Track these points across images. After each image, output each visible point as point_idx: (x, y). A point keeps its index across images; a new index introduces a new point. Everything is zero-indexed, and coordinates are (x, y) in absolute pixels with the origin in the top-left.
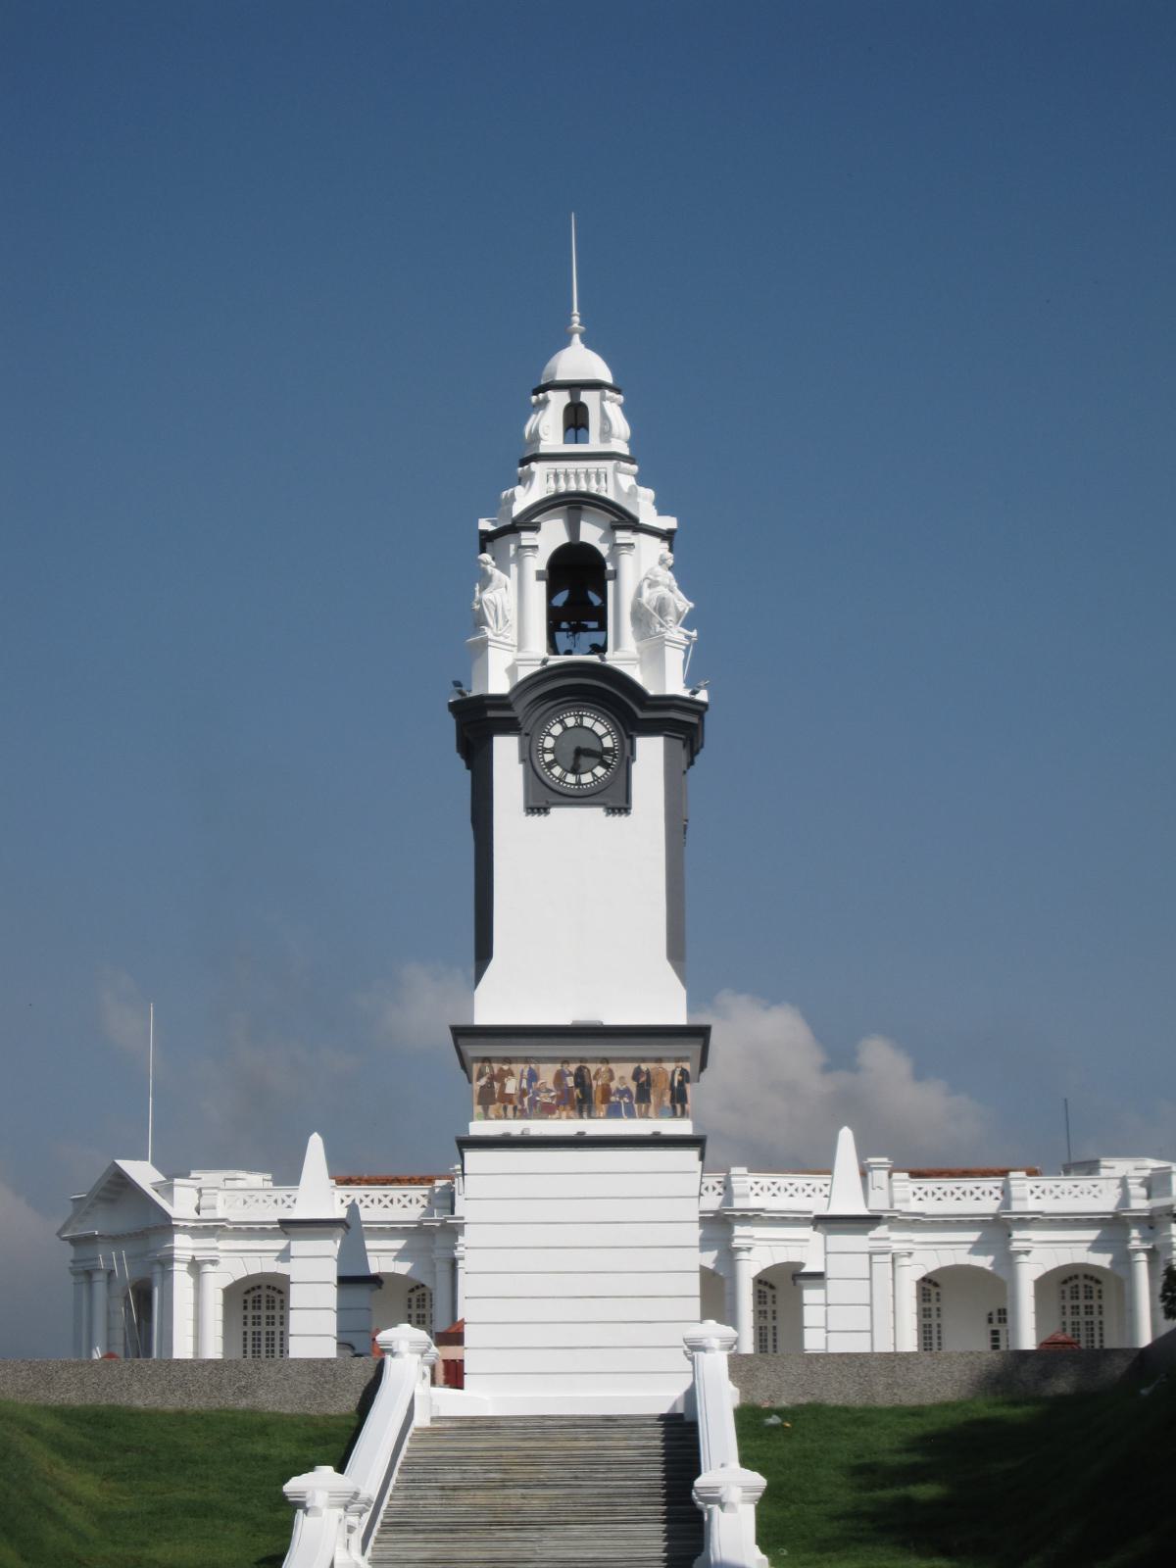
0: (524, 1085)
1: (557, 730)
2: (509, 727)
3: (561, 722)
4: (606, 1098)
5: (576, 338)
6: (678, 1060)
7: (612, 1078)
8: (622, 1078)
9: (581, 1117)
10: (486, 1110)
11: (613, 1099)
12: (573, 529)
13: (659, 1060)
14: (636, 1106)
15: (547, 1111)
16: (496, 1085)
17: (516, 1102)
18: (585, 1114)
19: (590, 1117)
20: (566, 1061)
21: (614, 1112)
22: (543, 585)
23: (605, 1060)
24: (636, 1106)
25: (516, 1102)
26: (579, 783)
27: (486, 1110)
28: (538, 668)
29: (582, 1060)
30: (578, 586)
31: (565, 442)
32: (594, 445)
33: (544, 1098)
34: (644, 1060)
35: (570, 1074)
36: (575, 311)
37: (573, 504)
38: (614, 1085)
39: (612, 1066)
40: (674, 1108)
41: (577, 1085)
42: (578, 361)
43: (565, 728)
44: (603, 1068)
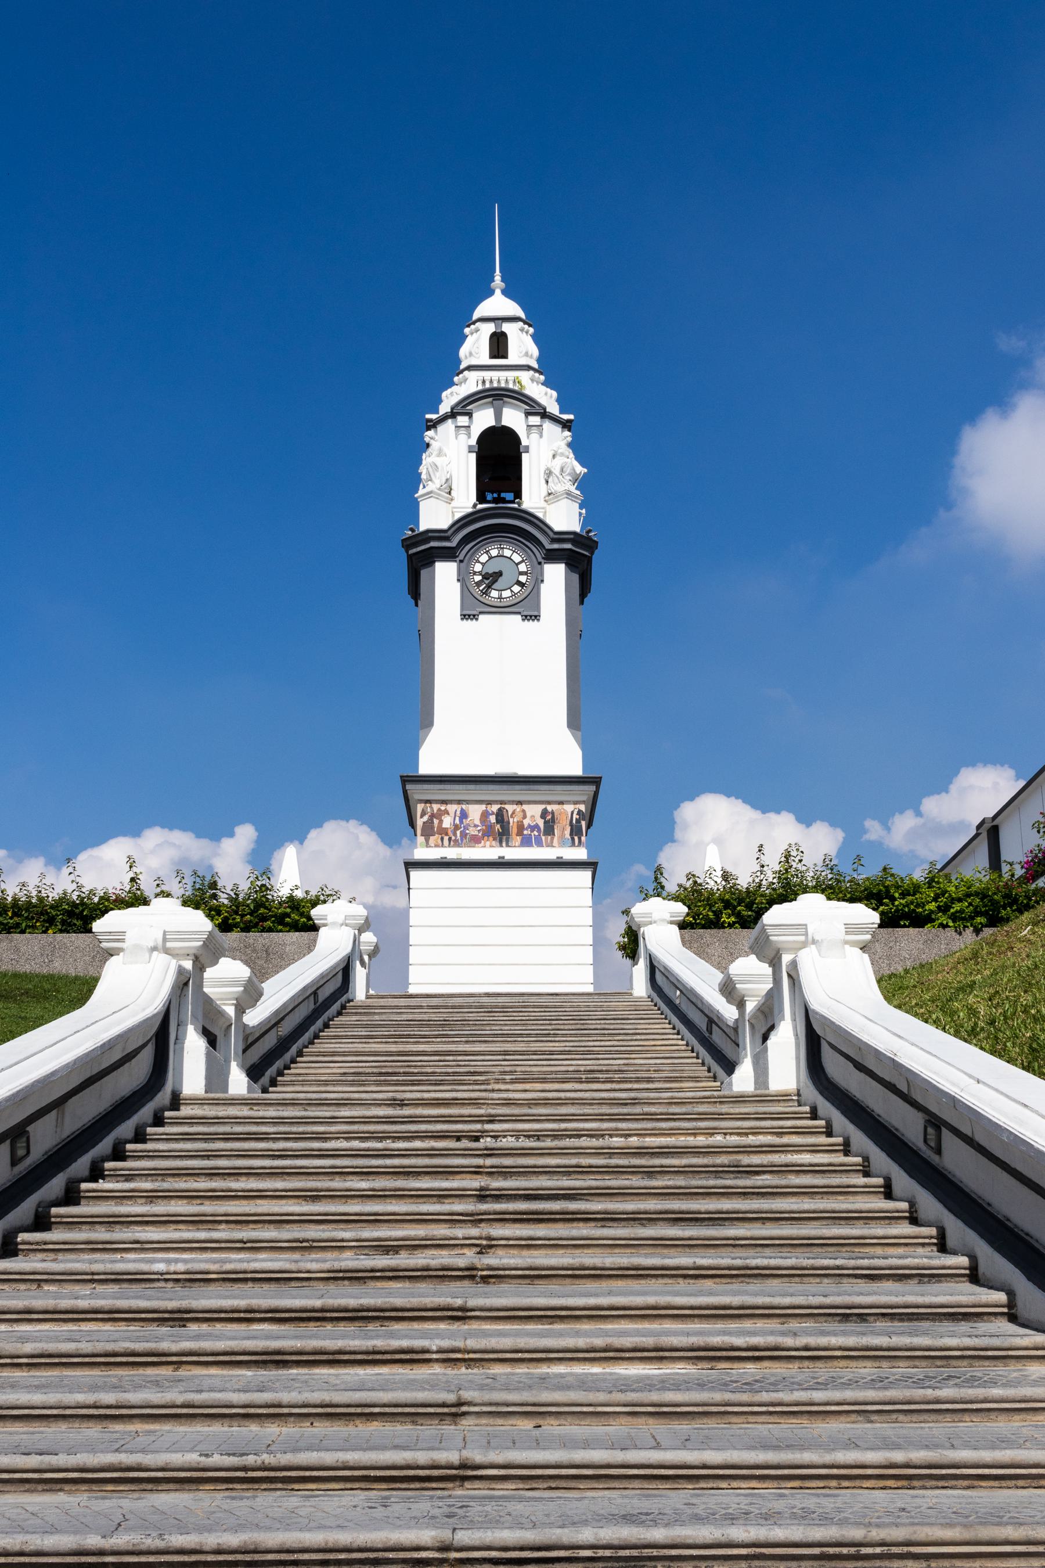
0: (457, 821)
1: (484, 558)
2: (449, 554)
3: (487, 552)
4: (520, 833)
5: (498, 292)
6: (576, 803)
7: (525, 817)
8: (533, 816)
9: (501, 846)
10: (427, 841)
11: (525, 832)
12: (498, 416)
13: (561, 803)
14: (543, 838)
15: (475, 840)
16: (436, 821)
17: (451, 834)
18: (504, 844)
19: (508, 845)
20: (489, 803)
21: (526, 842)
22: (474, 455)
23: (520, 803)
24: (543, 838)
25: (451, 834)
26: (500, 598)
27: (427, 841)
28: (471, 510)
29: (502, 802)
30: (499, 460)
31: (493, 356)
33: (472, 831)
34: (549, 803)
35: (493, 813)
36: (498, 278)
37: (497, 396)
38: (526, 822)
39: (525, 807)
40: (573, 839)
41: (497, 822)
42: (498, 304)
44: (518, 808)
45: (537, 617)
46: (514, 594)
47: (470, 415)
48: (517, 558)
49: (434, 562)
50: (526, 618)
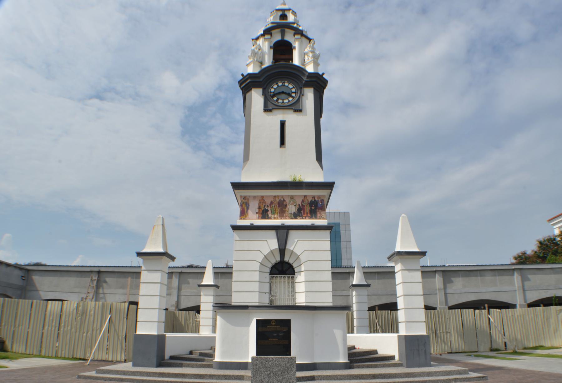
3: (277, 84)
22: (272, 50)
26: (283, 102)
31: (280, 19)
43: (278, 86)
45: (300, 111)
46: (289, 101)
48: (291, 86)
49: (251, 90)
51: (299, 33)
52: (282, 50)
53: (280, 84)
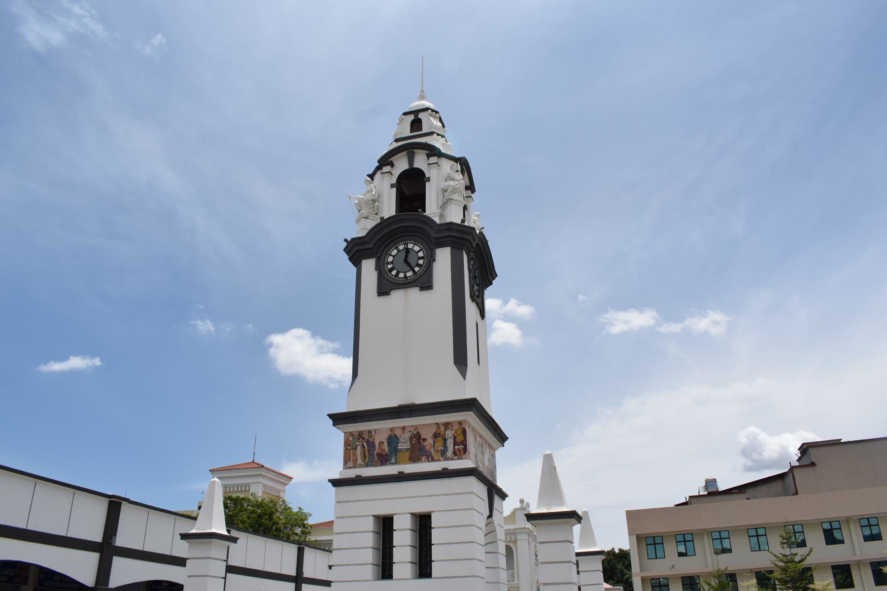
3: (397, 248)
12: (411, 161)
22: (394, 190)
26: (405, 277)
32: (425, 130)
47: (392, 165)
48: (417, 248)
49: (361, 261)
50: (422, 289)
51: (433, 152)
52: (411, 189)
53: (401, 247)
